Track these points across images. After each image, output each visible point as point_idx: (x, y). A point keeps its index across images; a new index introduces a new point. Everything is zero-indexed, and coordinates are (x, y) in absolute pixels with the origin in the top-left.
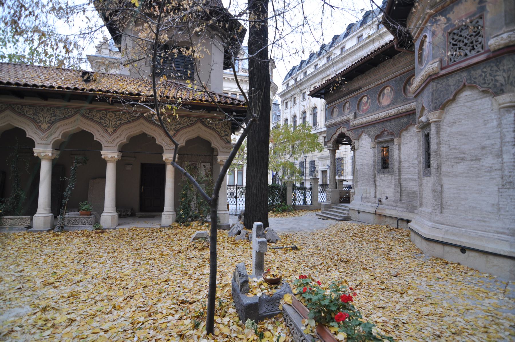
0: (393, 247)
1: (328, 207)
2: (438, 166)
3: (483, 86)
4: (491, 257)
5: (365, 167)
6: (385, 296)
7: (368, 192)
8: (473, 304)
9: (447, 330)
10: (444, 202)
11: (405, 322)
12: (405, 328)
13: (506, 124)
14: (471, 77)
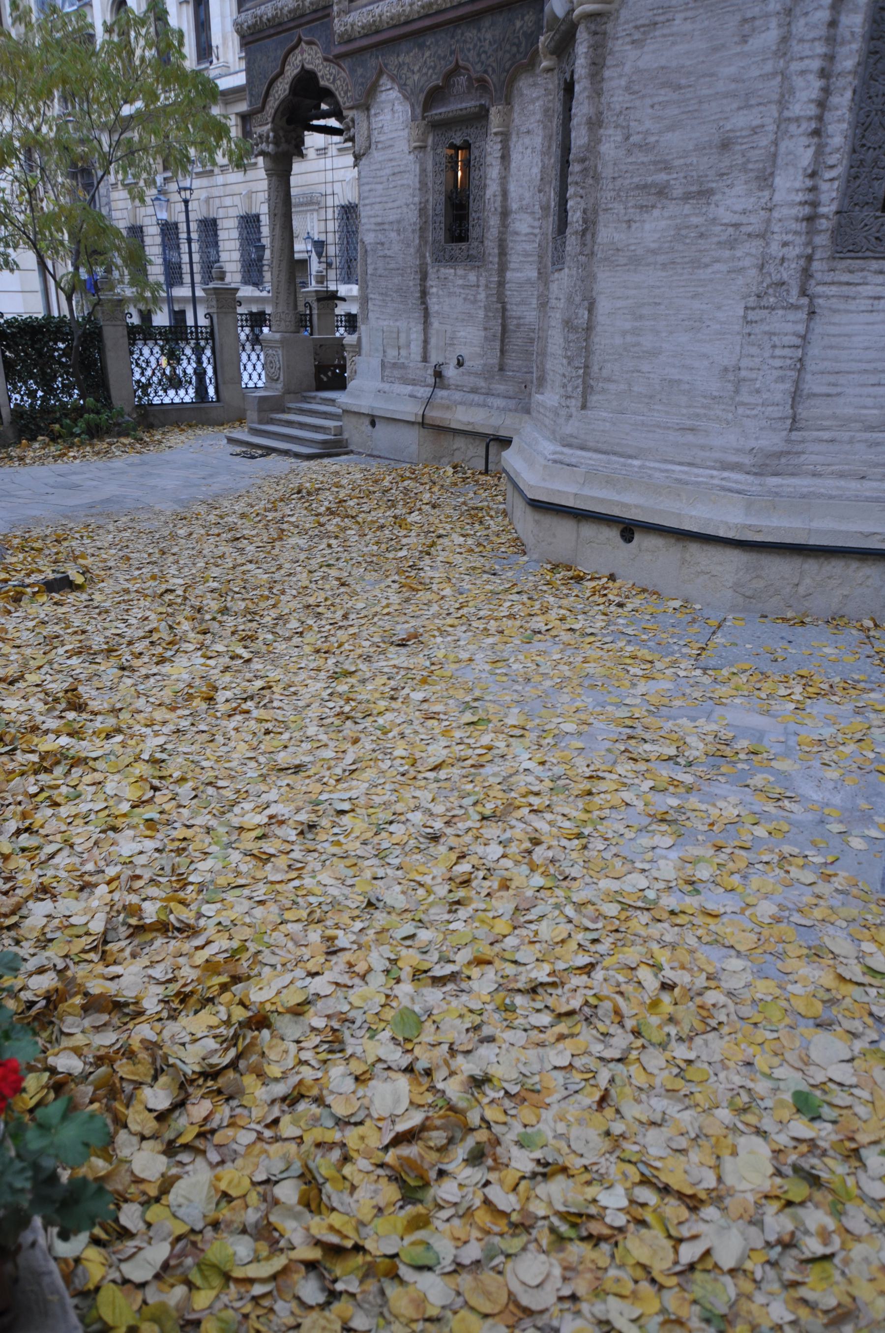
0: (441, 540)
1: (270, 407)
2: (585, 221)
4: (694, 548)
5: (393, 235)
8: (598, 704)
9: (471, 810)
10: (595, 368)
11: (346, 806)
12: (336, 830)
13: (801, 40)
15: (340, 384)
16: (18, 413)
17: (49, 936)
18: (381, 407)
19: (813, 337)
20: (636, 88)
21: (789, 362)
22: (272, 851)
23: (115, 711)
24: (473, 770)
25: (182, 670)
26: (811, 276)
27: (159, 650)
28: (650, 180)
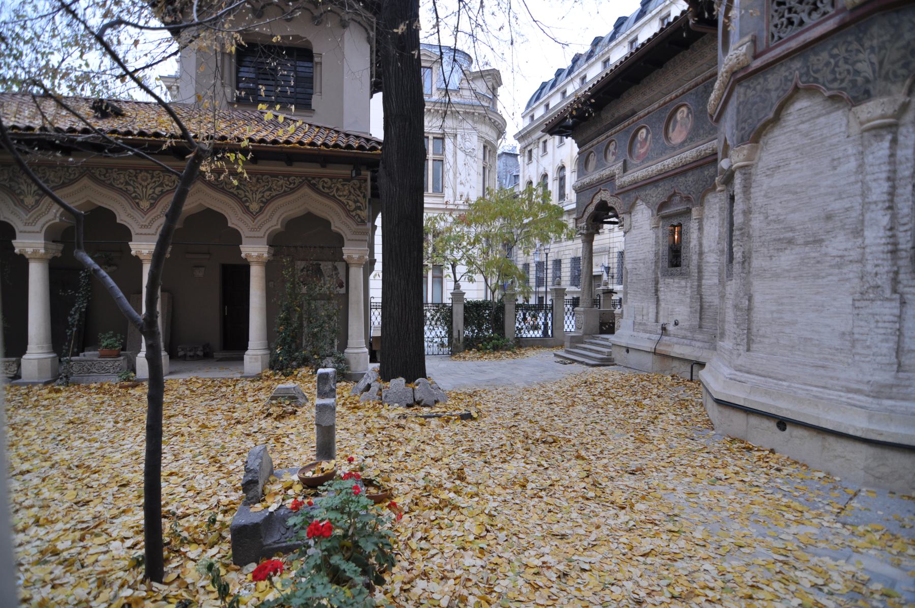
0: (661, 416)
1: (576, 341)
2: (744, 257)
3: (831, 86)
4: (831, 440)
6: (585, 512)
7: (645, 312)
8: (761, 535)
9: (665, 589)
10: (755, 330)
11: (587, 567)
12: (579, 581)
13: (872, 165)
14: (808, 70)
16: (466, 339)
17: (422, 601)
18: (632, 343)
20: (770, 195)
21: (889, 331)
22: (541, 584)
23: (478, 484)
24: (669, 562)
25: (514, 468)
26: (899, 282)
27: (504, 455)
28: (782, 236)
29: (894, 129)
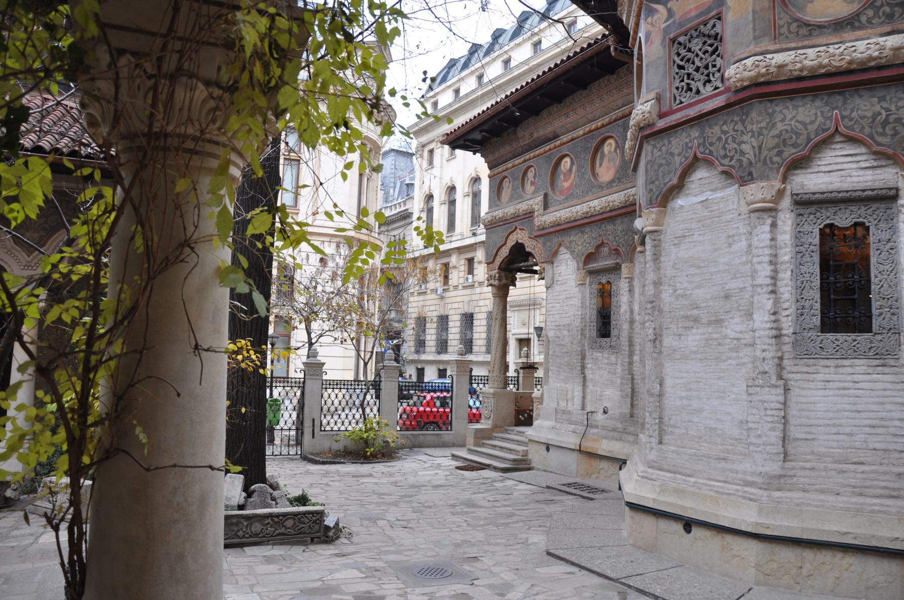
2: (655, 335)
4: (729, 538)
5: (566, 332)
7: (570, 395)
10: (666, 419)
13: (757, 248)
15: (529, 422)
19: (791, 404)
21: (776, 419)
28: (689, 313)
29: (773, 214)
